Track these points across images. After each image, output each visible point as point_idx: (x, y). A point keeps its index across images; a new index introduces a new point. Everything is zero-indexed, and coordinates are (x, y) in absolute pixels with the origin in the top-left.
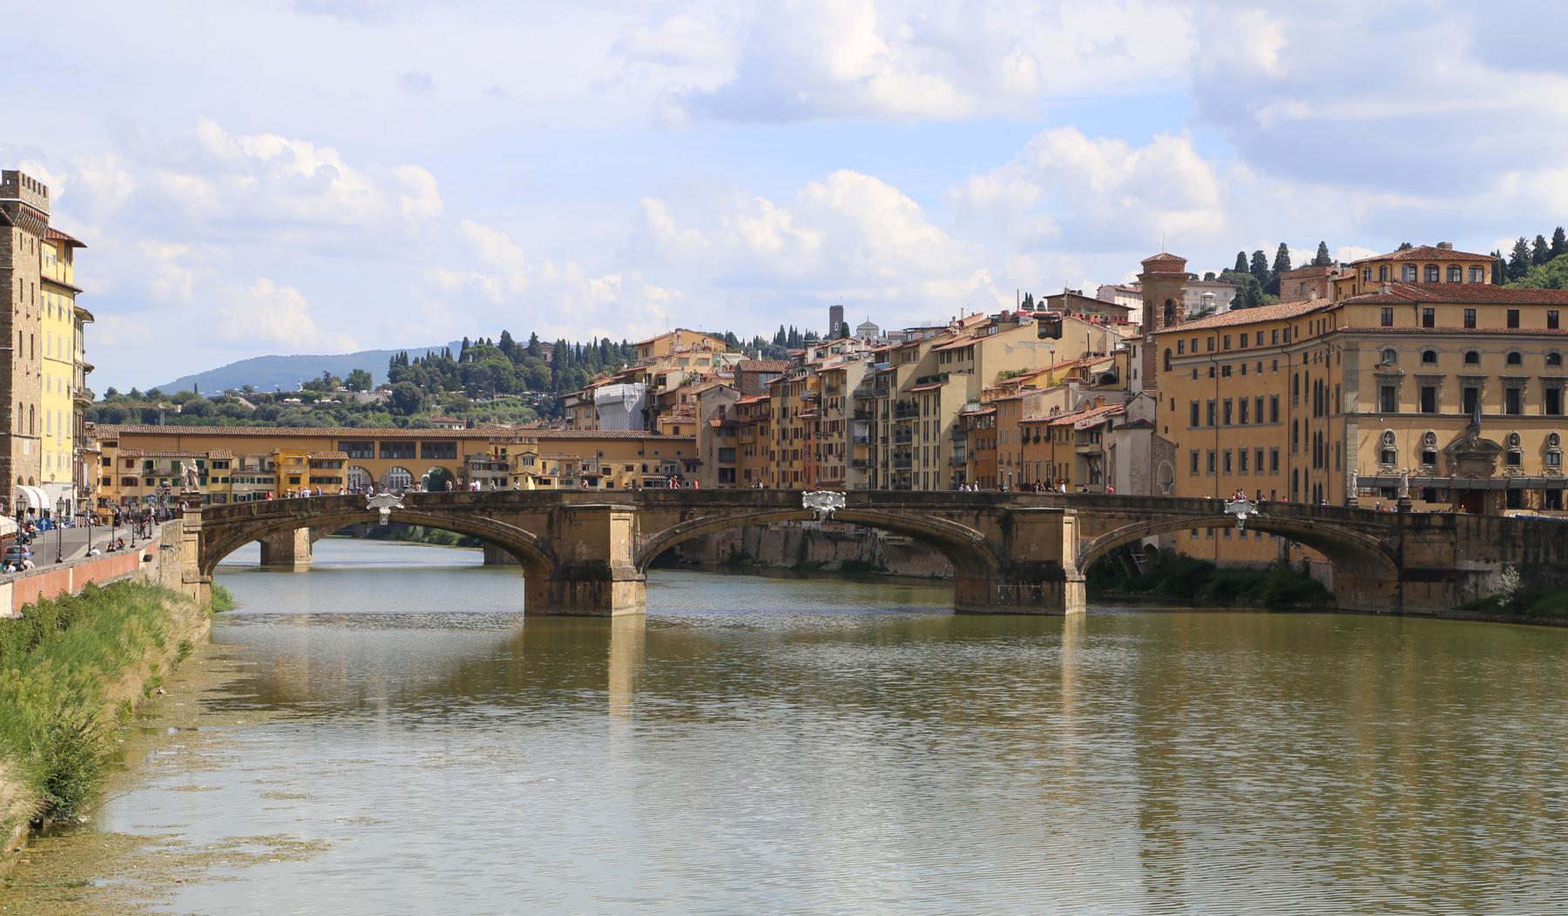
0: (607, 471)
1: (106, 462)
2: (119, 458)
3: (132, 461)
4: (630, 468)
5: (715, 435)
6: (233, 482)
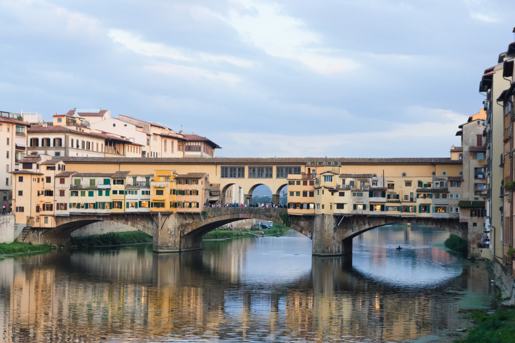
0: (391, 186)
1: (49, 180)
2: (56, 177)
3: (64, 179)
4: (408, 184)
5: (471, 158)
6: (126, 193)
